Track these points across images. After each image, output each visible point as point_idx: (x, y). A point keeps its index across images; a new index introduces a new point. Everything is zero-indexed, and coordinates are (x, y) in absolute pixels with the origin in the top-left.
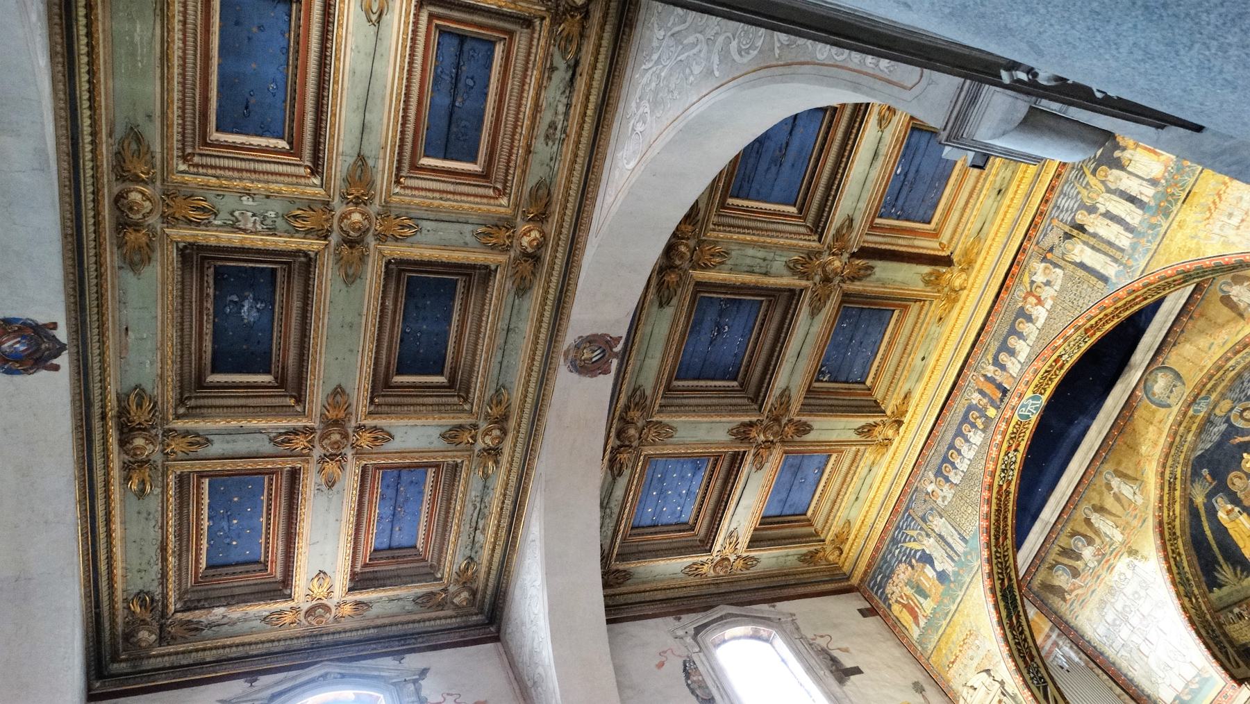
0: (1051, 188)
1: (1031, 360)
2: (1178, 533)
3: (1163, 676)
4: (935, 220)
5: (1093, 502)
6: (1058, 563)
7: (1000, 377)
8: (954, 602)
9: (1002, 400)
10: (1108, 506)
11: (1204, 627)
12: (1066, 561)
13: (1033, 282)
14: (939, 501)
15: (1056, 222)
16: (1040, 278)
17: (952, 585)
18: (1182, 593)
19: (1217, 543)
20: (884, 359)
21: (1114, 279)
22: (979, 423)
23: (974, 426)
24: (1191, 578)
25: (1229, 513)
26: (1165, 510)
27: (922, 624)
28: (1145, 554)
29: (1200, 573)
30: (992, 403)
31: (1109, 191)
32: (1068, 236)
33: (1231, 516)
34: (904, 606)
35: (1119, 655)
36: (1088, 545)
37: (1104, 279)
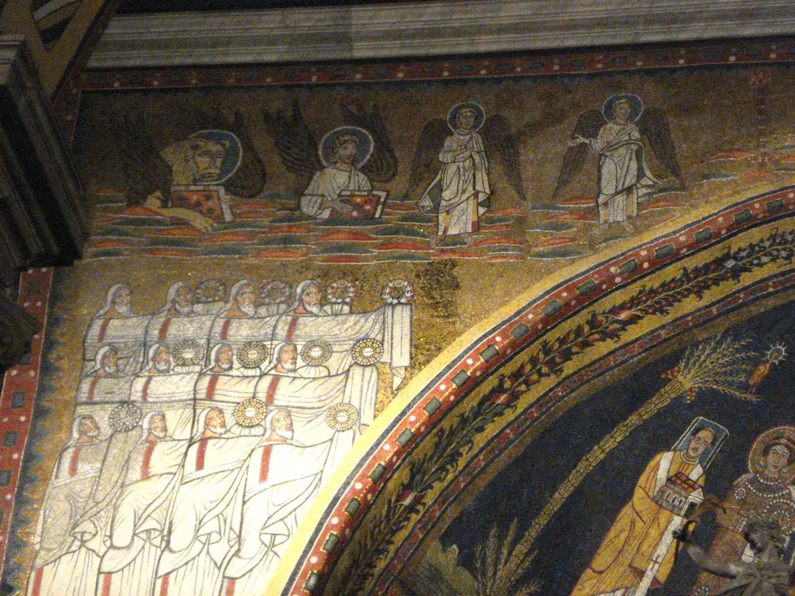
2: (569, 367)
3: (122, 536)
5: (509, 114)
6: (238, 126)
10: (528, 155)
11: (355, 563)
12: (263, 143)
18: (418, 454)
19: (578, 492)
24: (462, 462)
25: (677, 479)
26: (634, 290)
28: (465, 301)
29: (481, 484)
33: (672, 494)
35: (82, 410)
36: (364, 170)
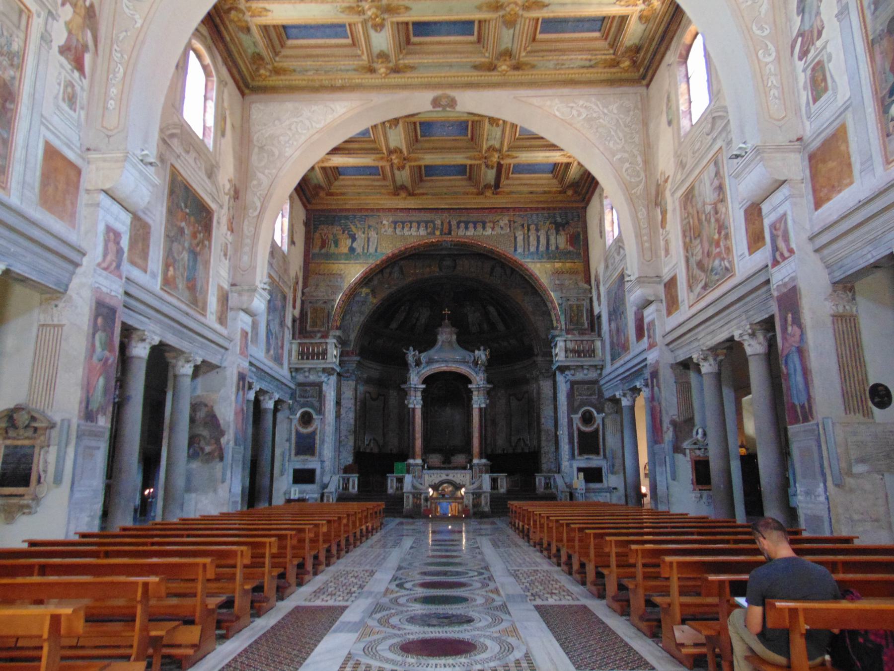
0: (537, 209)
1: (467, 237)
4: (514, 176)
7: (454, 227)
8: (346, 260)
9: (445, 234)
13: (498, 221)
14: (383, 230)
15: (525, 218)
16: (502, 223)
17: (352, 256)
20: (442, 180)
21: (517, 252)
22: (429, 230)
23: (426, 227)
27: (323, 251)
30: (442, 230)
31: (547, 233)
32: (523, 226)
34: (322, 239)
37: (515, 250)
